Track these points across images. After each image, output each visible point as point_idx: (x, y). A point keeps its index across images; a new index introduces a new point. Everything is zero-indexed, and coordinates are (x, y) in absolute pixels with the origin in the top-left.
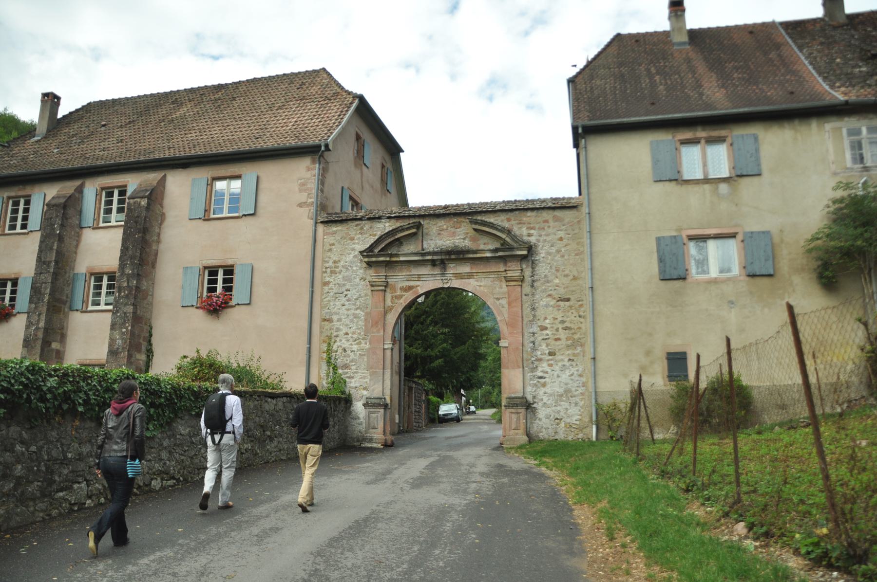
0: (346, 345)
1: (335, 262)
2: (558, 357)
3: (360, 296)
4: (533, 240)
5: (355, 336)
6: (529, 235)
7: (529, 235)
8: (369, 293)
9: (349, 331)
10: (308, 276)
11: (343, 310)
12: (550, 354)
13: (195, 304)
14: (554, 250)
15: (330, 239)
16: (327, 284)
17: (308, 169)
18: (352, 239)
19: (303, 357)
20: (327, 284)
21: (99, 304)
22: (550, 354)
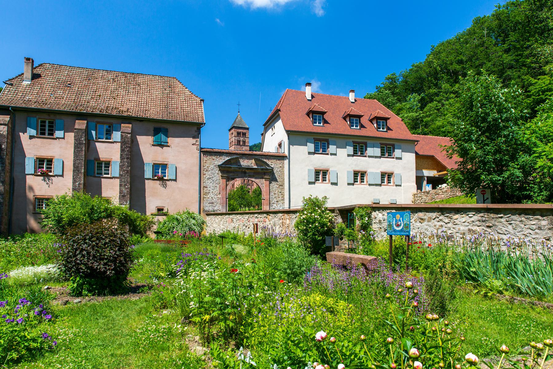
0: (213, 196)
1: (207, 167)
2: (279, 203)
3: (217, 180)
4: (272, 166)
5: (216, 193)
6: (271, 165)
7: (271, 165)
8: (220, 178)
9: (214, 191)
10: (198, 171)
11: (211, 184)
12: (277, 202)
13: (151, 178)
14: (278, 170)
15: (205, 159)
16: (205, 174)
17: (196, 131)
18: (214, 160)
19: (198, 199)
20: (205, 174)
21: (108, 174)
22: (277, 202)
